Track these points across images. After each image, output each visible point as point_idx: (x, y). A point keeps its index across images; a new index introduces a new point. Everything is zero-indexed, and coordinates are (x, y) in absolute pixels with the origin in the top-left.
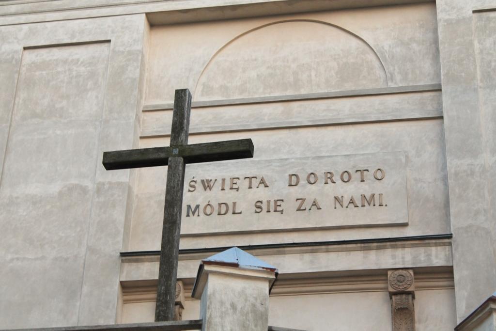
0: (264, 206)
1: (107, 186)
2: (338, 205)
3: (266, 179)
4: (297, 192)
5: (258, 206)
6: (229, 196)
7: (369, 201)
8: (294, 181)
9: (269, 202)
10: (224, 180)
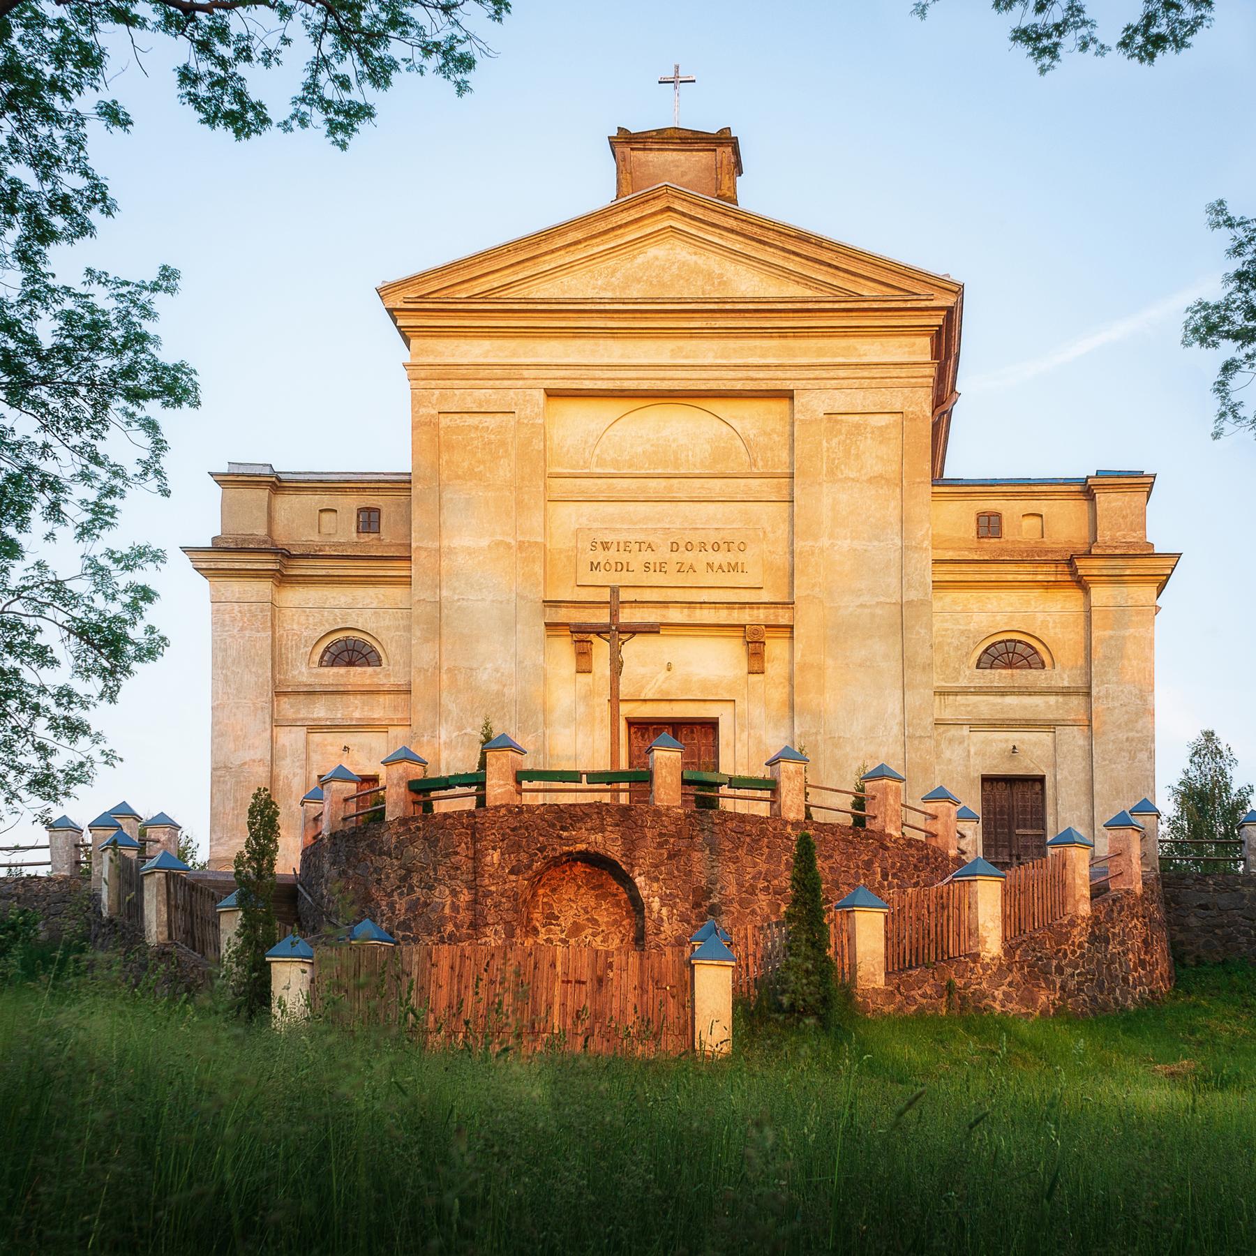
0: (652, 567)
1: (526, 544)
2: (710, 570)
3: (652, 544)
5: (647, 566)
6: (624, 557)
7: (733, 568)
8: (674, 547)
9: (655, 563)
10: (618, 543)
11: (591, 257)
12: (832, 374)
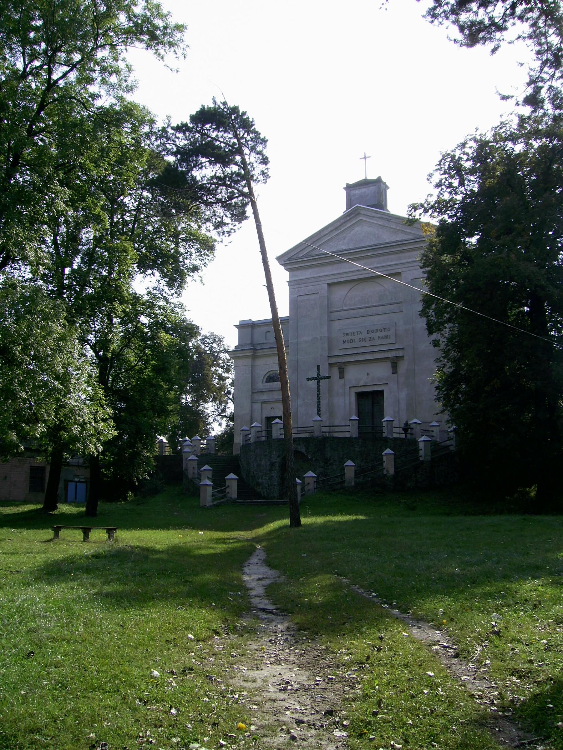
4: (368, 335)
6: (352, 337)
7: (386, 337)
8: (368, 332)
11: (337, 235)
12: (413, 265)
